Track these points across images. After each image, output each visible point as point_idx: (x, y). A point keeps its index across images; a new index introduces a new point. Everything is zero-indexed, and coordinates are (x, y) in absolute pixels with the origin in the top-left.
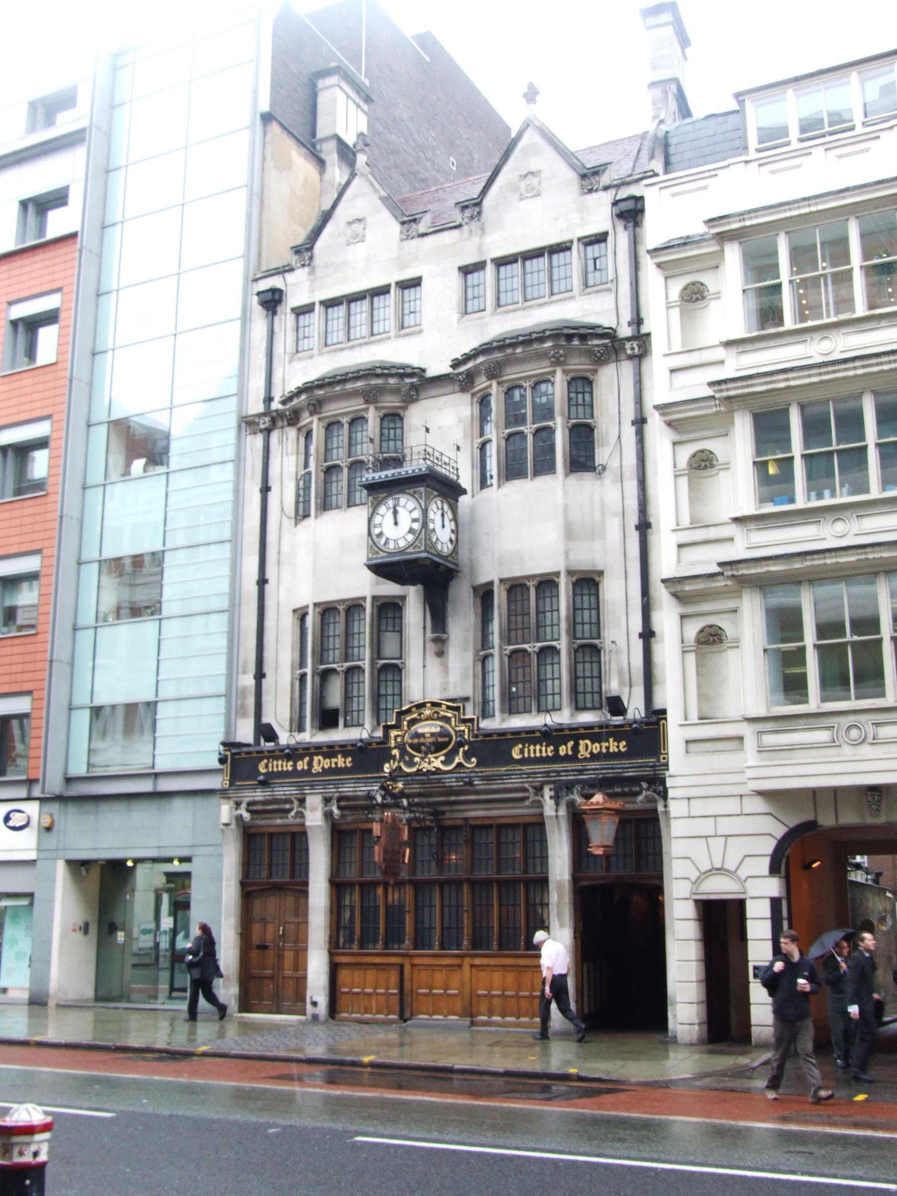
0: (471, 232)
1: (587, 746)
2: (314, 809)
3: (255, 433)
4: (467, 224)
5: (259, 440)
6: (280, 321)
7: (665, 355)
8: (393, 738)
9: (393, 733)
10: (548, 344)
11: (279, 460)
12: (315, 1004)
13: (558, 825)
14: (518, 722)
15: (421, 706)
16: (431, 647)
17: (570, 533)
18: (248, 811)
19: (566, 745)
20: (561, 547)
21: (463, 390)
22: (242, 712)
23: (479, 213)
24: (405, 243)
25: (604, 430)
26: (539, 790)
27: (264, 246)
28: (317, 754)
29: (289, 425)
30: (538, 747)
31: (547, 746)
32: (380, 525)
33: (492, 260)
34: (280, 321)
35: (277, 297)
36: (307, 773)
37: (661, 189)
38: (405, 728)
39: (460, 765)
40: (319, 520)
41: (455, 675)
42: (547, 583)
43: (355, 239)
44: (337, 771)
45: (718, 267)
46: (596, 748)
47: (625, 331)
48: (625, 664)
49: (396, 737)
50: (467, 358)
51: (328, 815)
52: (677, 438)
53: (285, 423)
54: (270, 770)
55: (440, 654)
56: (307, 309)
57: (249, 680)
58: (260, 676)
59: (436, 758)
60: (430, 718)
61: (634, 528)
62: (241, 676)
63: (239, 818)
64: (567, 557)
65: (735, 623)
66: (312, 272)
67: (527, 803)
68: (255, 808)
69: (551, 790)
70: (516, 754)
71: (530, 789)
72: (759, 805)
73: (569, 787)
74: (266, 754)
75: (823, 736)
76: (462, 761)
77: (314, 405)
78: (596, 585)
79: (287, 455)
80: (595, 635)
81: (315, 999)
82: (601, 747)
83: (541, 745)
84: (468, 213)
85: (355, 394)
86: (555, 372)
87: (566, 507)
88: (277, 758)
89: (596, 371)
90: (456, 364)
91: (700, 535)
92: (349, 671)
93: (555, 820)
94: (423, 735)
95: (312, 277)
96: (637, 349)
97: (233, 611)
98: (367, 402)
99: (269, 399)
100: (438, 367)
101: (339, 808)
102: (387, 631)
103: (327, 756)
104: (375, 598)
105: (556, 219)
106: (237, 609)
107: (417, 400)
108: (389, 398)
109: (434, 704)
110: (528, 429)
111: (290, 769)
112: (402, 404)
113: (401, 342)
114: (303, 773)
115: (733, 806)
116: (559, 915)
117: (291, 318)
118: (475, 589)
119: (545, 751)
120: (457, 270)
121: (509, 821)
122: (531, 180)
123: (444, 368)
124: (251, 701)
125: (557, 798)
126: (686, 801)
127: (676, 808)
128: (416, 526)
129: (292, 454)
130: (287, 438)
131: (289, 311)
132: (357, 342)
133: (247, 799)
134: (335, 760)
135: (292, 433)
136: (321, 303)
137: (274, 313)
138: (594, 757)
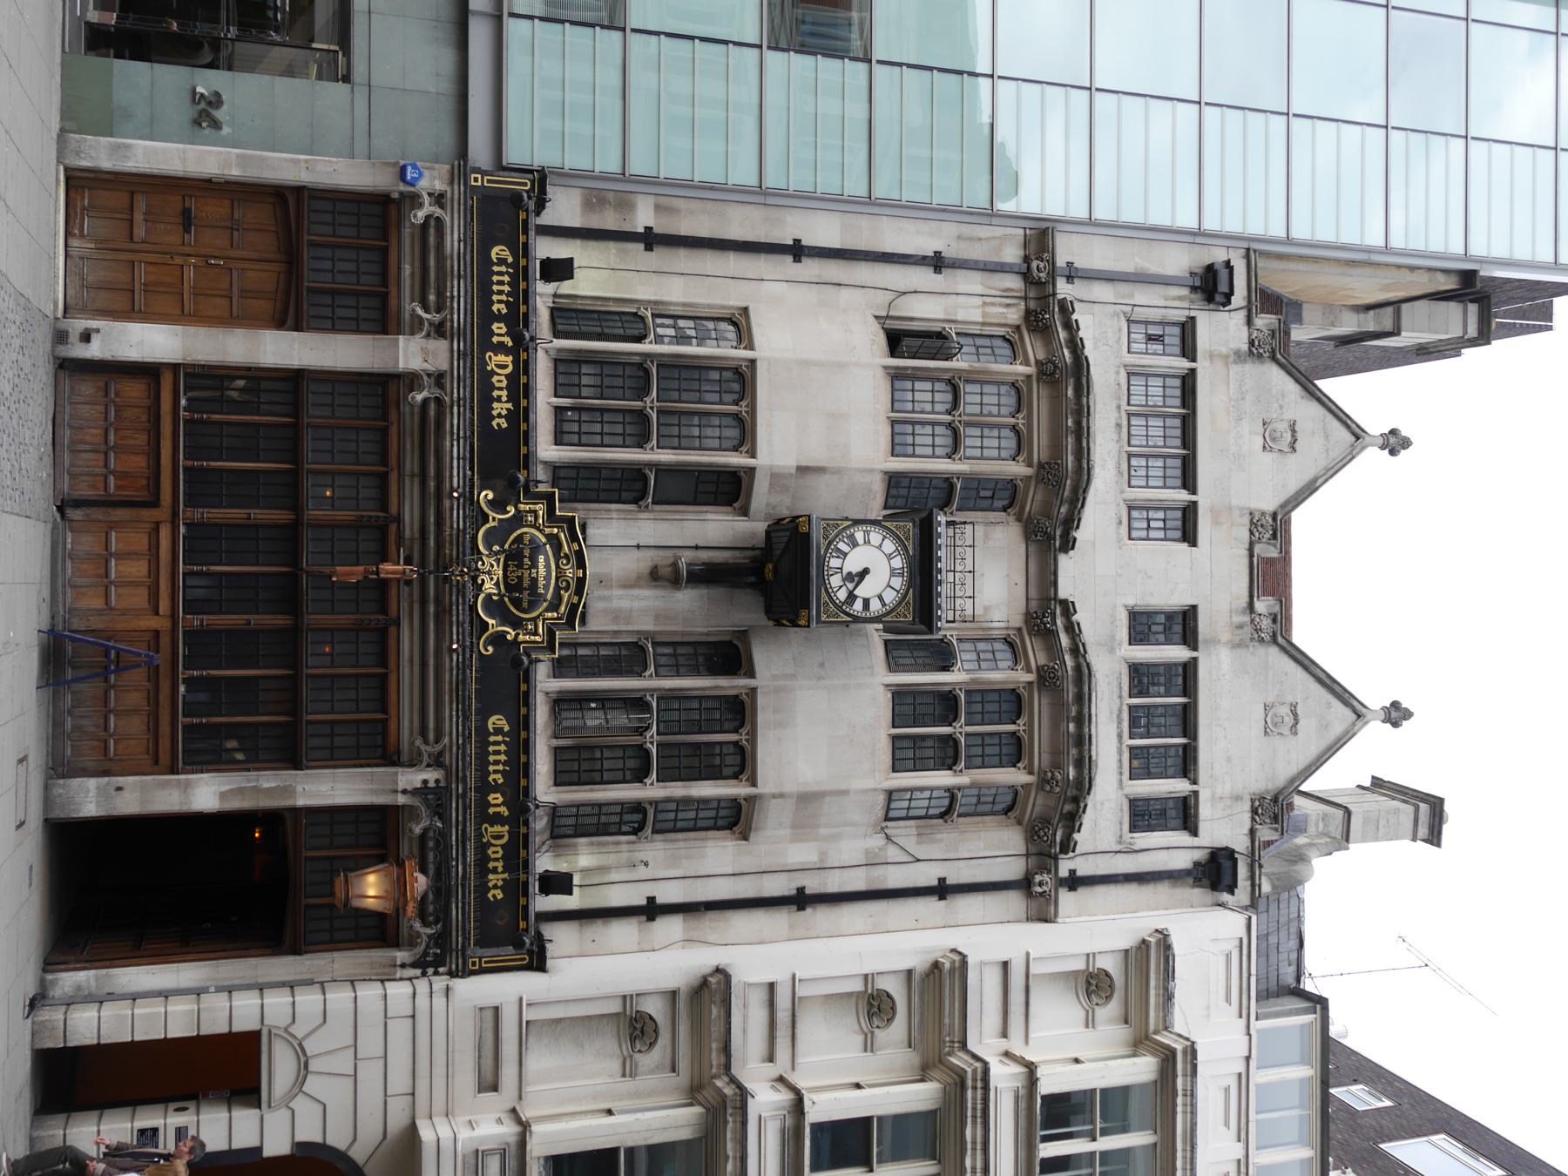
0: (1240, 626)
1: (500, 837)
2: (424, 351)
3: (1025, 245)
4: (1252, 621)
6: (1180, 298)
7: (1028, 954)
9: (540, 508)
10: (1072, 773)
11: (979, 289)
12: (86, 337)
13: (383, 792)
14: (541, 714)
15: (581, 564)
16: (664, 558)
17: (807, 799)
18: (428, 217)
19: (503, 804)
20: (790, 788)
21: (1029, 617)
22: (594, 200)
23: (1262, 640)
24: (1246, 520)
25: (939, 836)
26: (437, 762)
27: (1292, 266)
28: (516, 362)
29: (1028, 312)
30: (503, 758)
31: (503, 773)
32: (867, 542)
33: (1195, 659)
34: (1180, 298)
35: (1218, 298)
36: (486, 344)
37: (1241, 939)
38: (547, 530)
40: (880, 373)
41: (622, 600)
42: (742, 763)
43: (1270, 435)
44: (487, 400)
45: (1126, 1022)
46: (496, 852)
47: (1064, 867)
48: (614, 877)
49: (535, 512)
51: (411, 380)
52: (916, 978)
53: (1032, 305)
54: (496, 268)
55: (654, 576)
56: (1188, 348)
57: (644, 217)
58: (650, 239)
59: (497, 584)
61: (799, 884)
62: (651, 200)
63: (414, 200)
64: (774, 796)
65: (657, 1069)
66: (1239, 357)
67: (419, 742)
68: (432, 231)
69: (437, 781)
70: (496, 721)
71: (438, 748)
72: (397, 1121)
73: (440, 811)
74: (523, 262)
76: (491, 631)
77: (1052, 375)
78: (730, 826)
79: (985, 304)
80: (658, 826)
81: (95, 338)
82: (497, 860)
83: (505, 763)
84: (1266, 623)
85: (1056, 447)
86: (1031, 773)
87: (844, 793)
88: (514, 283)
89: (1019, 823)
90: (1068, 608)
91: (783, 1016)
92: (641, 417)
93: (391, 787)
94: (534, 565)
96: (1038, 889)
97: (762, 194)
98: (1041, 466)
99: (1072, 275)
100: (1072, 575)
101: (426, 401)
103: (513, 379)
104: (751, 471)
105: (1229, 760)
106: (760, 199)
109: (581, 582)
110: (960, 729)
111: (495, 308)
112: (1026, 515)
114: (487, 333)
115: (399, 1080)
116: (240, 791)
117: (1181, 316)
118: (744, 635)
121: (393, 697)
122: (1289, 720)
123: (1066, 589)
124: (609, 221)
125: (423, 791)
126: (411, 1014)
127: (398, 991)
128: (858, 605)
129: (984, 315)
130: (1008, 305)
131: (1193, 314)
132: (1125, 423)
133: (448, 220)
134: (504, 399)
135: (1014, 315)
136: (1193, 371)
138: (482, 848)
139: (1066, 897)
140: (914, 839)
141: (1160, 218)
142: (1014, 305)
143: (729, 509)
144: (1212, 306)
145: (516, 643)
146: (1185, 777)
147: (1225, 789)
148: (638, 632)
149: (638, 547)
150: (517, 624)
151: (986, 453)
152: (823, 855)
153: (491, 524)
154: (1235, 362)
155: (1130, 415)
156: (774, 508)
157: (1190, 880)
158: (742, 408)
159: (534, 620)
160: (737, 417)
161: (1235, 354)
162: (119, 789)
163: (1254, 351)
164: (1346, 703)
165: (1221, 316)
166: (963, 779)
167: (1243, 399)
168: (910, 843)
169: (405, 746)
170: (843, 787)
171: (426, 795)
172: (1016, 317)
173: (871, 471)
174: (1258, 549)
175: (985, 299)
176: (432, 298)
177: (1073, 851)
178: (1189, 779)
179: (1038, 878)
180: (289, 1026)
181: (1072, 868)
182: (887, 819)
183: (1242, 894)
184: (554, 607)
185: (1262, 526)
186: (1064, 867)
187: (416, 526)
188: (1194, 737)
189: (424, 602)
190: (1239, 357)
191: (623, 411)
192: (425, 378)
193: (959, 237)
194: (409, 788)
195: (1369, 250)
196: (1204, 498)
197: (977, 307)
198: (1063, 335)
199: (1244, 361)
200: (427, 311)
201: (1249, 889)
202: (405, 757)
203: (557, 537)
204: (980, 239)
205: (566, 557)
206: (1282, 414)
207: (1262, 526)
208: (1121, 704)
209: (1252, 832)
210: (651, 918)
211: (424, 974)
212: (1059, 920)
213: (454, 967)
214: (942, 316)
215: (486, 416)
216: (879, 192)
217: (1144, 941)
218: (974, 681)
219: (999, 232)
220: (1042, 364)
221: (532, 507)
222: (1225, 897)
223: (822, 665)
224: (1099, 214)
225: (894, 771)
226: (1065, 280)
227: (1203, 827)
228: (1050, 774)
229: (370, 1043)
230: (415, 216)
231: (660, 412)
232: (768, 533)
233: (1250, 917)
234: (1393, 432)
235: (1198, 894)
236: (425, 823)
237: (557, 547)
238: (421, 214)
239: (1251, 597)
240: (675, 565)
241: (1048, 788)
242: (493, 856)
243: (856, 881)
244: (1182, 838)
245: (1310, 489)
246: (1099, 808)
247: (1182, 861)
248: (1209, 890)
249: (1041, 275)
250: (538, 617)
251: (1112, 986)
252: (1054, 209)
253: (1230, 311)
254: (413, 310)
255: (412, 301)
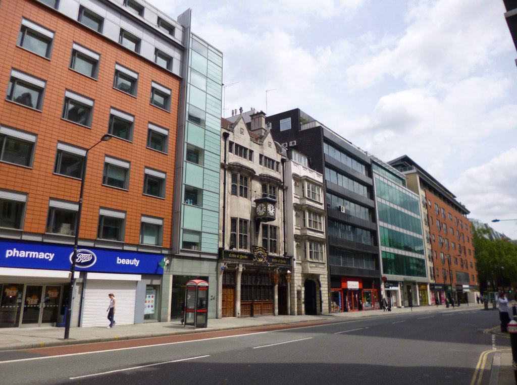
57: (221, 232)
58: (224, 231)
75: (314, 265)
99: (225, 161)
119: (276, 261)
124: (222, 237)
127: (295, 274)
215: (246, 259)
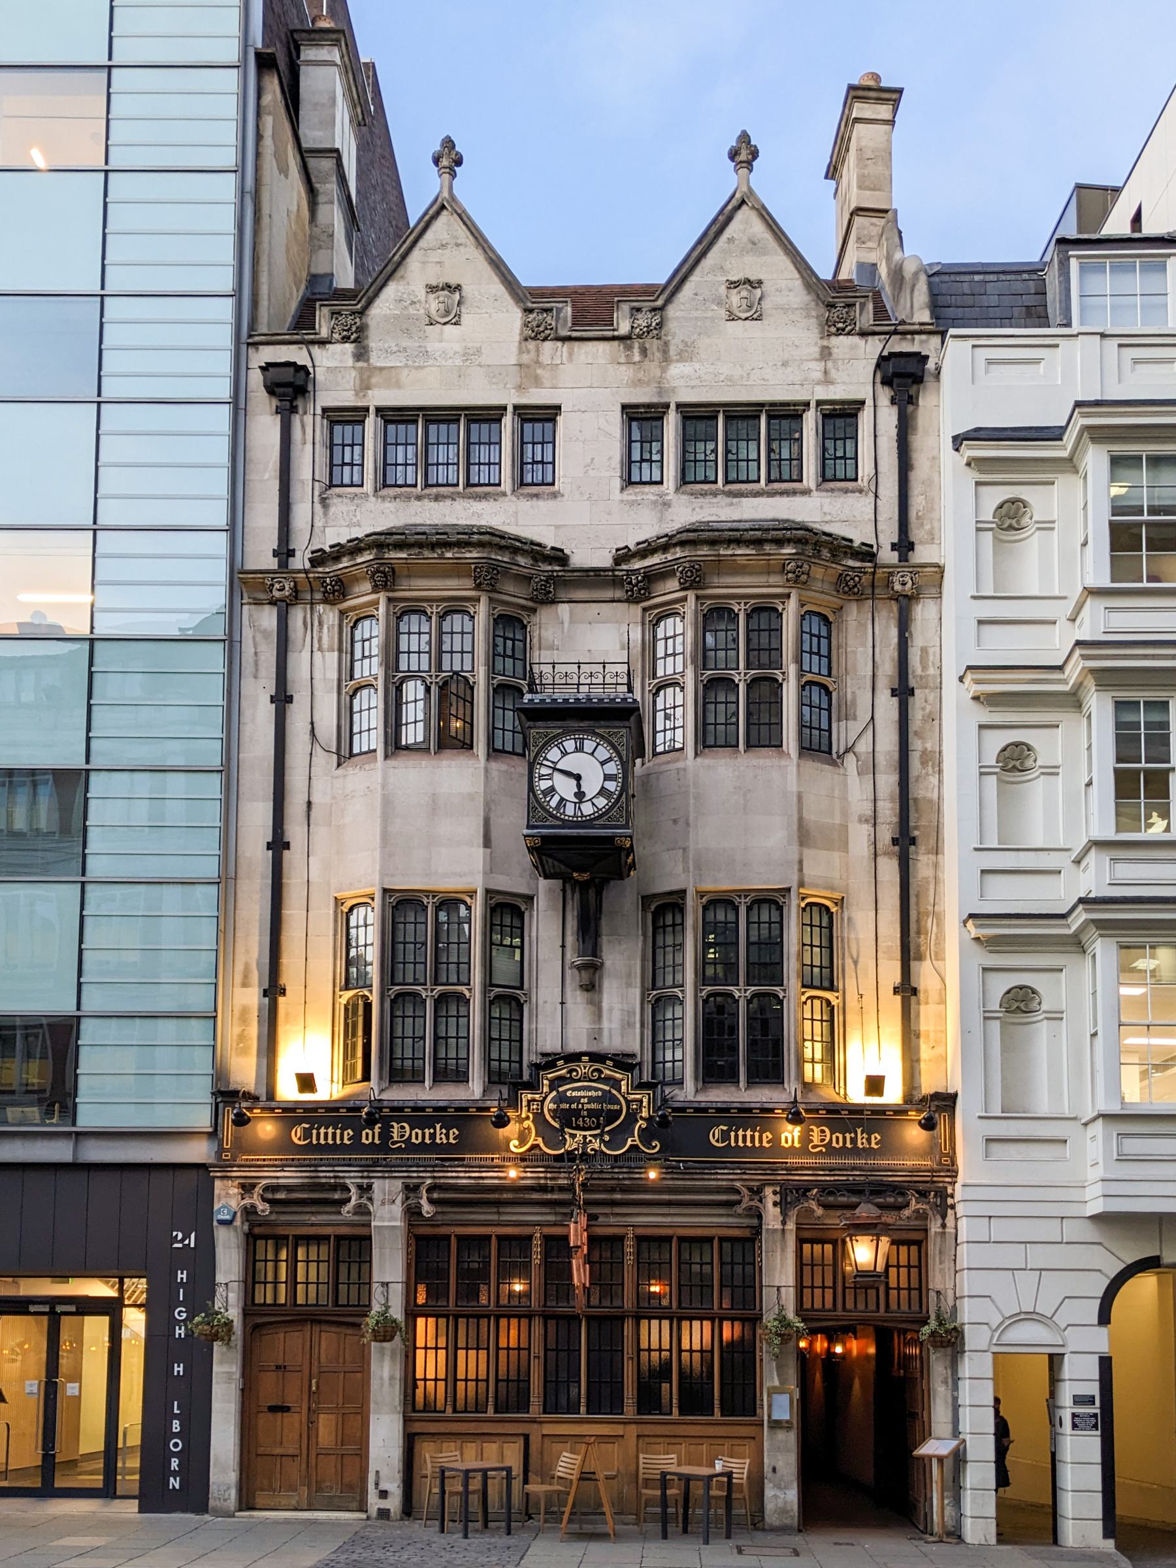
0: (644, 351)
3: (258, 603)
4: (639, 337)
5: (268, 618)
8: (525, 1103)
11: (306, 654)
14: (719, 1095)
15: (575, 1057)
17: (804, 836)
18: (264, 1200)
21: (631, 600)
23: (660, 325)
24: (531, 345)
26: (757, 1192)
27: (264, 290)
29: (325, 601)
38: (546, 1089)
39: (634, 1148)
49: (529, 1101)
50: (647, 549)
51: (412, 1213)
53: (318, 596)
55: (591, 987)
60: (585, 1078)
63: (249, 1212)
67: (739, 1209)
69: (775, 1193)
71: (745, 1191)
76: (638, 1142)
79: (320, 649)
86: (788, 596)
90: (625, 555)
93: (779, 1235)
95: (360, 364)
96: (909, 585)
99: (284, 552)
101: (431, 1201)
102: (501, 945)
107: (554, 602)
108: (510, 587)
112: (530, 604)
113: (525, 505)
117: (321, 424)
120: (619, 408)
123: (603, 560)
125: (784, 1205)
129: (331, 650)
130: (321, 624)
131: (319, 411)
133: (264, 1182)
135: (330, 616)
136: (379, 410)
137: (294, 410)
139: (922, 554)
140: (850, 723)
141: (220, 450)
142: (320, 617)
143: (527, 915)
144: (310, 388)
145: (649, 1119)
146: (801, 416)
147: (815, 370)
148: (642, 1003)
149: (562, 1003)
150: (632, 1117)
151: (468, 648)
152: (862, 820)
153: (540, 1141)
154: (367, 361)
155: (427, 485)
156: (525, 870)
157: (910, 408)
158: (430, 902)
159: (628, 1102)
160: (438, 908)
161: (358, 360)
162: (774, 1470)
163: (357, 336)
164: (729, 219)
165: (320, 375)
166: (792, 669)
167: (405, 349)
168: (855, 727)
169: (746, 1221)
170: (795, 799)
171: (787, 1203)
172: (331, 615)
173: (486, 770)
174: (564, 332)
175: (315, 649)
176: (337, 1196)
177: (872, 546)
178: (804, 411)
179: (898, 587)
180: (990, 1328)
181: (889, 547)
182: (830, 753)
183: (927, 346)
184: (616, 1084)
185: (538, 326)
186: (887, 556)
187: (547, 1210)
188: (762, 405)
189: (614, 1203)
190: (361, 355)
191: (436, 1017)
192: (409, 1202)
193: (256, 677)
194: (781, 1218)
195: (242, 192)
196: (510, 398)
197: (323, 657)
198: (345, 562)
199: (364, 348)
200: (349, 1200)
201: (924, 337)
202: (755, 1222)
203: (551, 1081)
204: (256, 653)
205: (570, 1072)
206: (419, 301)
207: (538, 326)
208: (724, 493)
209: (863, 334)
210: (915, 991)
211: (953, 1207)
212: (941, 563)
213: (947, 1179)
214: (335, 695)
216: (216, 762)
217: (968, 464)
218: (694, 661)
219: (248, 633)
220: (376, 586)
221: (525, 1103)
222: (930, 365)
223: (675, 821)
224: (222, 520)
225: (781, 746)
226: (291, 559)
227: (859, 396)
228: (790, 575)
229: (1013, 1256)
230: (263, 1211)
231: (436, 983)
232: (546, 877)
233: (952, 336)
234: (436, 161)
235: (926, 401)
236: (813, 1205)
237: (562, 1080)
238: (262, 1206)
239: (614, 338)
240: (579, 968)
241: (804, 577)
242: (841, 1144)
243: (888, 781)
244: (865, 419)
245: (498, 265)
246: (828, 518)
247: (889, 417)
248: (922, 386)
249: (287, 588)
250: (625, 1099)
251: (1013, 501)
252: (220, 572)
253: (314, 366)
254: (348, 1212)
255: (340, 1213)
